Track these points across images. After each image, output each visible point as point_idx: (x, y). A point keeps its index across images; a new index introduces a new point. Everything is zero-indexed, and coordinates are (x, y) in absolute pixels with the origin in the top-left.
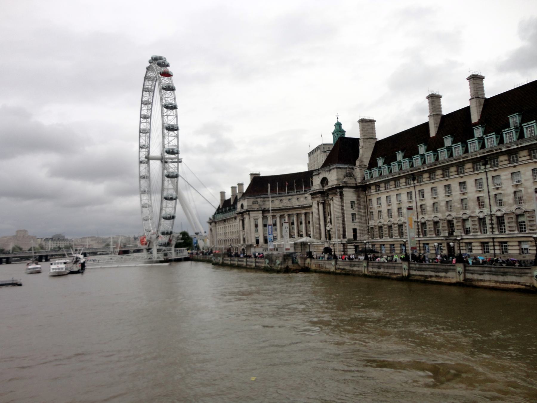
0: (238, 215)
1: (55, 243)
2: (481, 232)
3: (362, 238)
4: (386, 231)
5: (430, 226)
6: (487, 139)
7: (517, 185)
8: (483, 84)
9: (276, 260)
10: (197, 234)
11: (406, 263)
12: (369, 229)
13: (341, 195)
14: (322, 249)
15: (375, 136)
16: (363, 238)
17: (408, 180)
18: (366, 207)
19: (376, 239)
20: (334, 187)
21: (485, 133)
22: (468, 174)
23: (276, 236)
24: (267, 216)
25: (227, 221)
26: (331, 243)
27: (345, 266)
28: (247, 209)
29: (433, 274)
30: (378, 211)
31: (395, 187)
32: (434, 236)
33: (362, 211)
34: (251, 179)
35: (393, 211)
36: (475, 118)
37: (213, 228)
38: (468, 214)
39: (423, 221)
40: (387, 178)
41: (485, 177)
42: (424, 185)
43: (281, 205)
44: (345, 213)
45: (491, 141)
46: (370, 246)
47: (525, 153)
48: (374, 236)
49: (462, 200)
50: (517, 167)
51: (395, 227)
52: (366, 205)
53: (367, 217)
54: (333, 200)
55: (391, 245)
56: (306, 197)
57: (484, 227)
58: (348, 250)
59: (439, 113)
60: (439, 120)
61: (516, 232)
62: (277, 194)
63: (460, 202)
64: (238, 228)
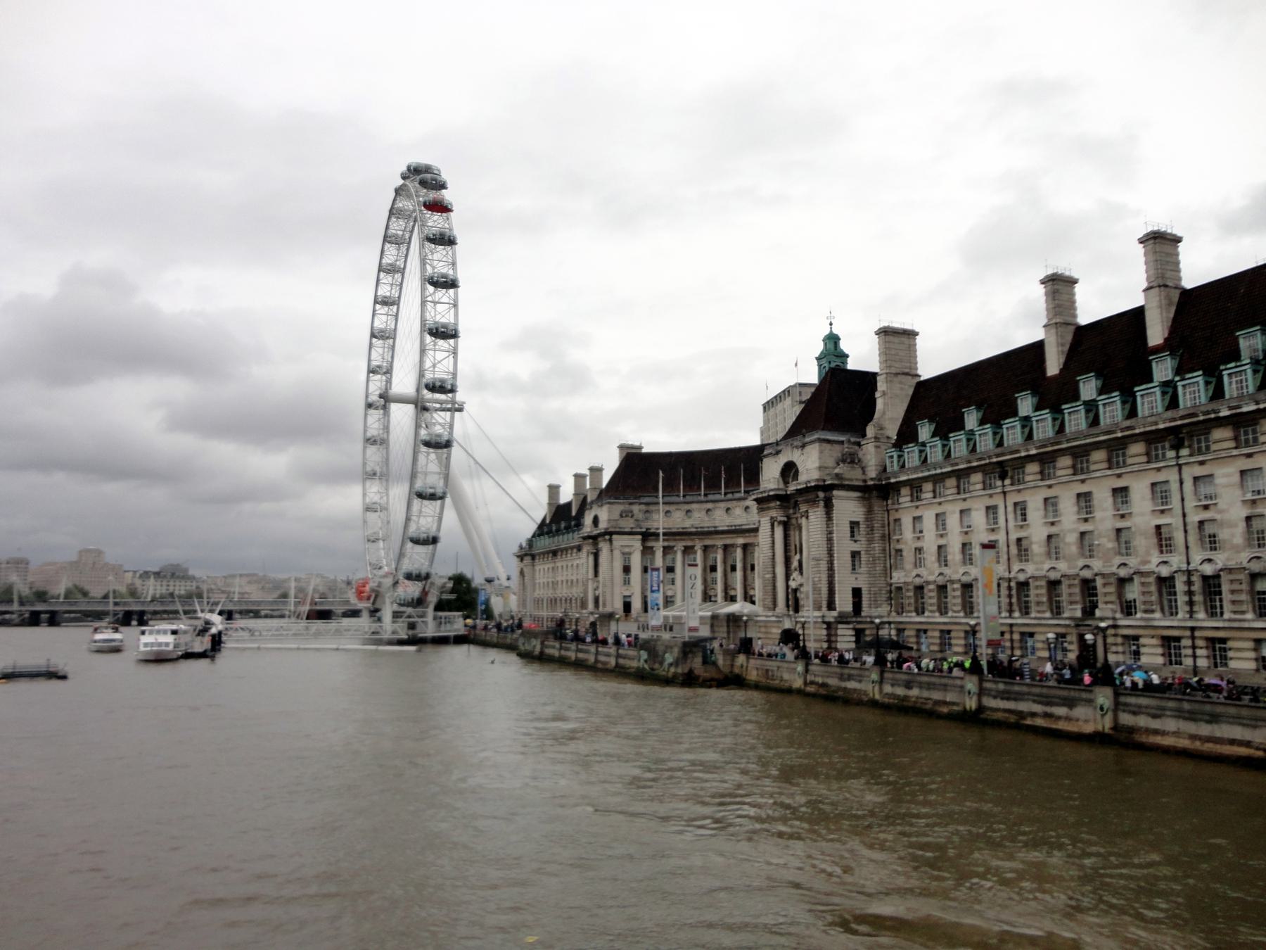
0: (586, 542)
1: (165, 583)
2: (1162, 610)
3: (874, 612)
4: (931, 597)
5: (1039, 592)
6: (1184, 386)
7: (1254, 502)
8: (1177, 255)
9: (665, 652)
10: (489, 581)
11: (975, 679)
12: (891, 592)
14: (776, 631)
15: (917, 369)
16: (877, 611)
17: (990, 479)
18: (887, 538)
19: (906, 617)
20: (811, 487)
21: (1180, 371)
22: (1135, 468)
23: (671, 597)
24: (652, 548)
25: (560, 553)
26: (798, 619)
27: (828, 677)
28: (608, 529)
29: (1038, 708)
30: (916, 549)
31: (958, 493)
32: (1048, 615)
33: (877, 546)
34: (620, 457)
35: (950, 550)
36: (1156, 334)
37: (525, 570)
38: (1132, 565)
39: (1022, 577)
40: (939, 471)
41: (1177, 477)
42: (1028, 491)
43: (688, 524)
44: (835, 548)
45: (1194, 391)
46: (893, 632)
48: (902, 608)
49: (1119, 531)
50: (1255, 456)
51: (954, 590)
52: (887, 532)
53: (888, 561)
54: (807, 518)
55: (942, 631)
56: (747, 508)
57: (1170, 601)
58: (839, 639)
59: (1069, 320)
60: (1069, 338)
61: (1250, 616)
62: (678, 496)
63: (1113, 535)
64: (584, 571)
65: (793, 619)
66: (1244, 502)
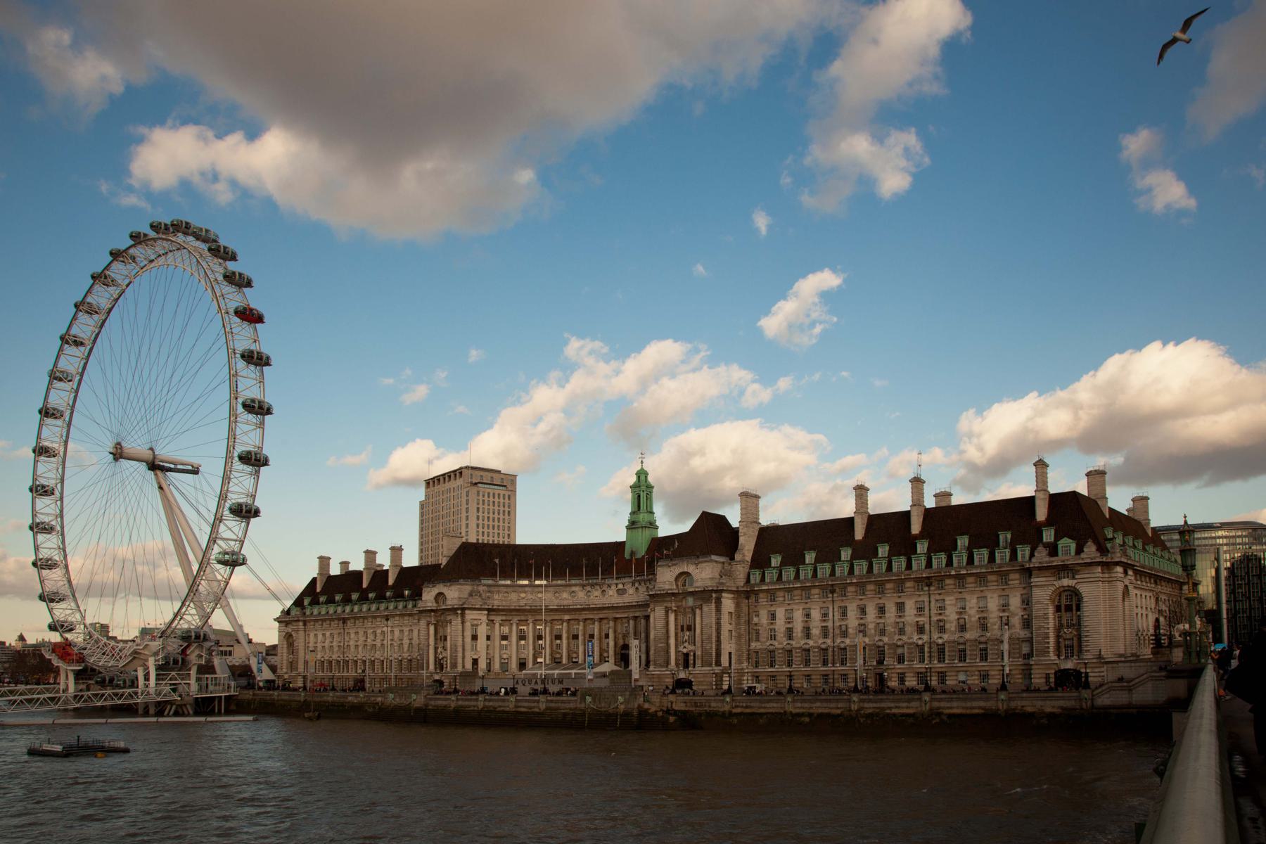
13: (719, 602)
14: (669, 681)
18: (749, 622)
24: (493, 620)
25: (352, 621)
28: (459, 605)
29: (892, 705)
33: (743, 627)
35: (794, 630)
39: (842, 646)
40: (791, 586)
47: (970, 579)
51: (796, 653)
52: (747, 619)
54: (701, 609)
56: (573, 592)
65: (687, 672)
66: (957, 613)
